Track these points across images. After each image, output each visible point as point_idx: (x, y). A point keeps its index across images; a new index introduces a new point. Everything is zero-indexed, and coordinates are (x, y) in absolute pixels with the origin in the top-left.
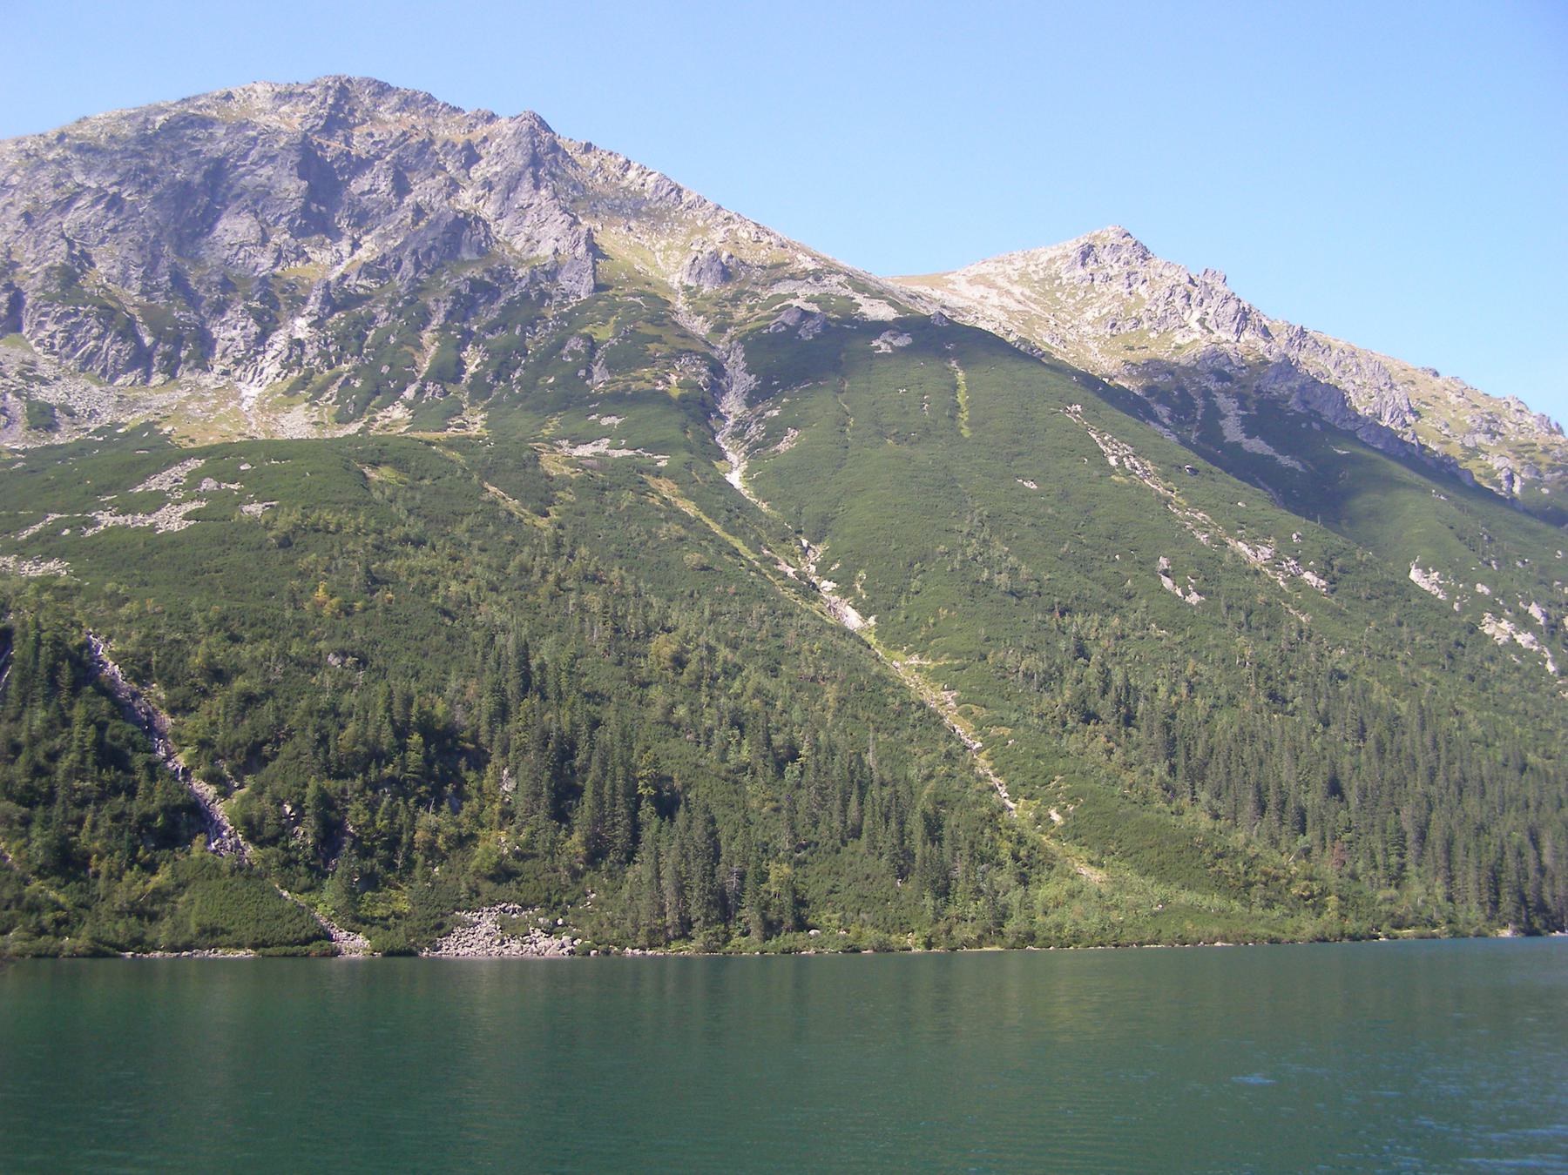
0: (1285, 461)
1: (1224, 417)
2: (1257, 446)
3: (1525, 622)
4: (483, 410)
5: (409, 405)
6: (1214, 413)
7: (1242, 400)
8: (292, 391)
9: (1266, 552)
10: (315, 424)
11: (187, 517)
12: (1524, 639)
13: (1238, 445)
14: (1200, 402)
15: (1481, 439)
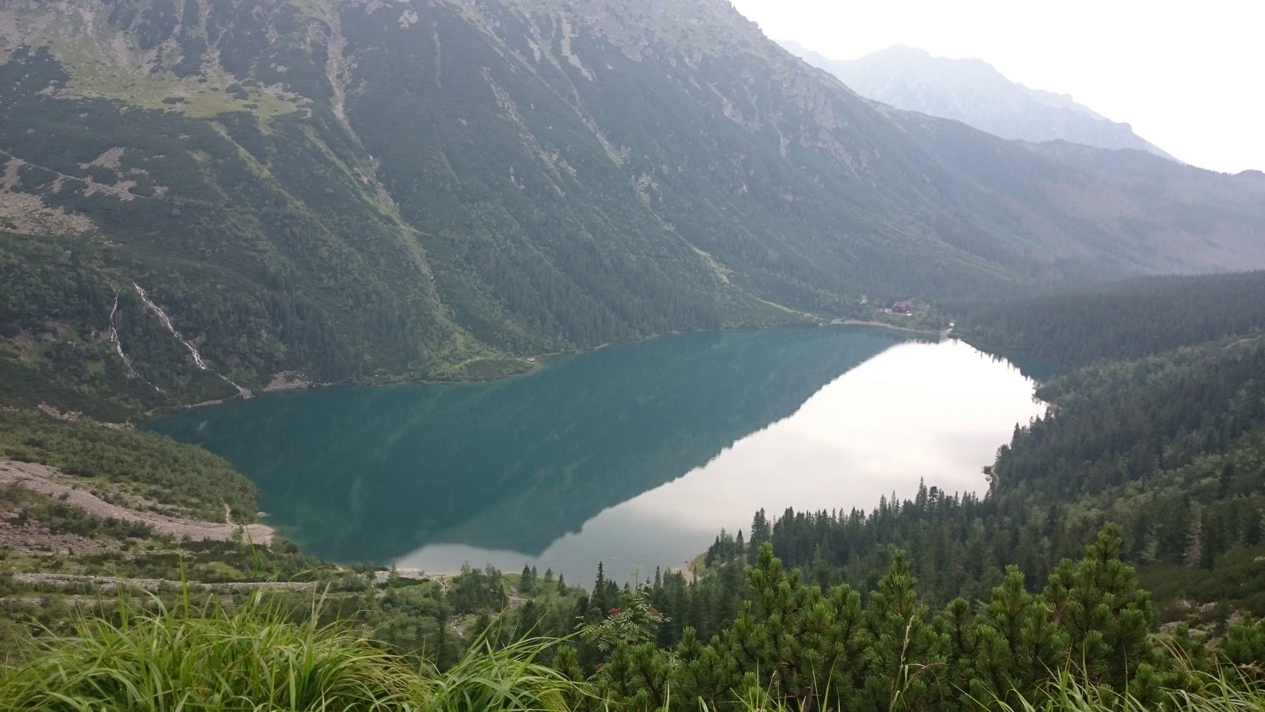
0: (585, 72)
1: (563, 37)
2: (574, 60)
3: (659, 176)
4: (218, 48)
5: (178, 40)
6: (560, 35)
7: (573, 24)
8: (112, 20)
9: (555, 157)
10: (131, 49)
11: (131, 190)
12: (655, 185)
13: (566, 58)
14: (555, 25)
15: (694, 21)
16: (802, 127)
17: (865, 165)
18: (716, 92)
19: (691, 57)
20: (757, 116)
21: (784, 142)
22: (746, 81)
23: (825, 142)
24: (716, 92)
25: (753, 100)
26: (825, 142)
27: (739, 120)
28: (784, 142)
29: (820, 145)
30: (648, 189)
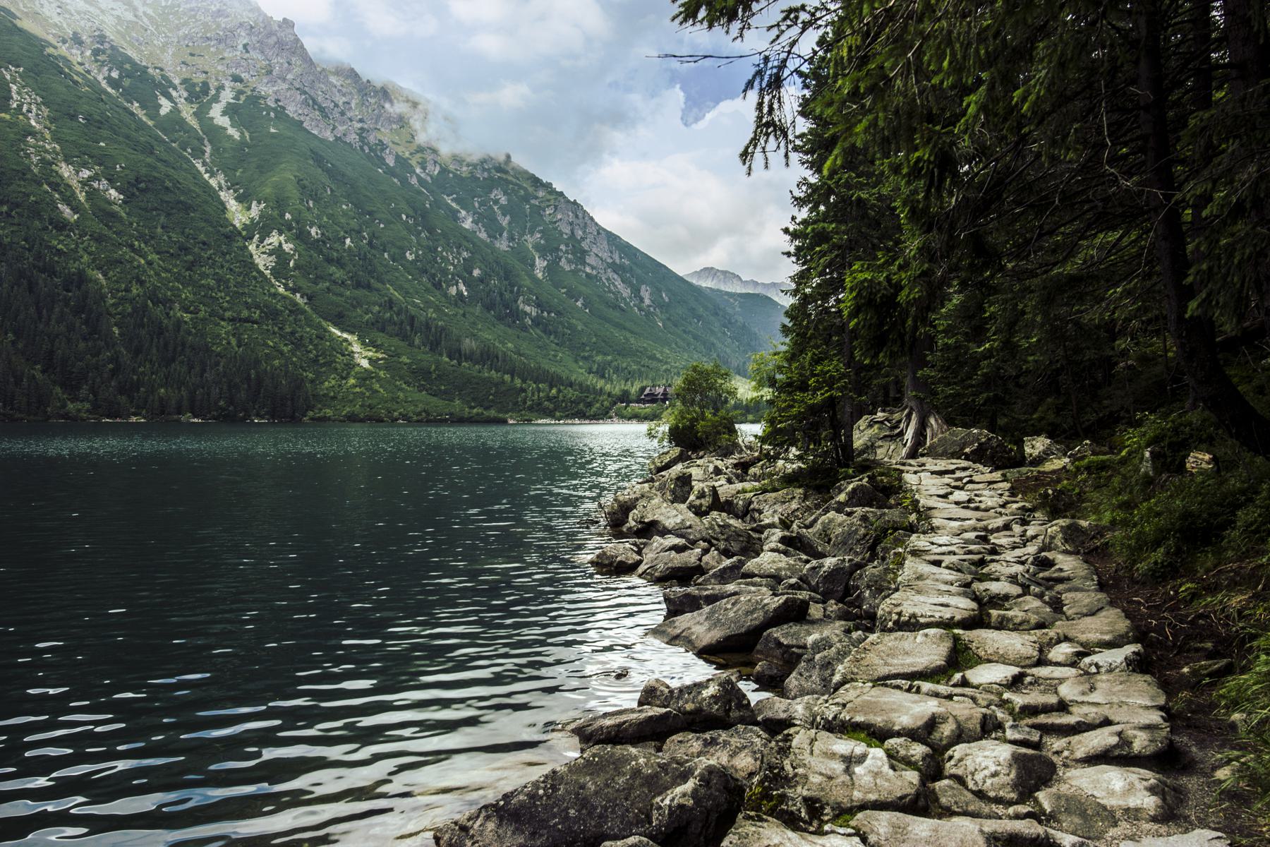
16: (563, 247)
17: (647, 302)
18: (454, 205)
19: (424, 168)
20: (505, 234)
21: (540, 264)
22: (496, 202)
23: (593, 268)
24: (454, 205)
25: (505, 221)
26: (593, 268)
27: (483, 235)
28: (540, 264)
29: (588, 270)
30: (278, 252)
